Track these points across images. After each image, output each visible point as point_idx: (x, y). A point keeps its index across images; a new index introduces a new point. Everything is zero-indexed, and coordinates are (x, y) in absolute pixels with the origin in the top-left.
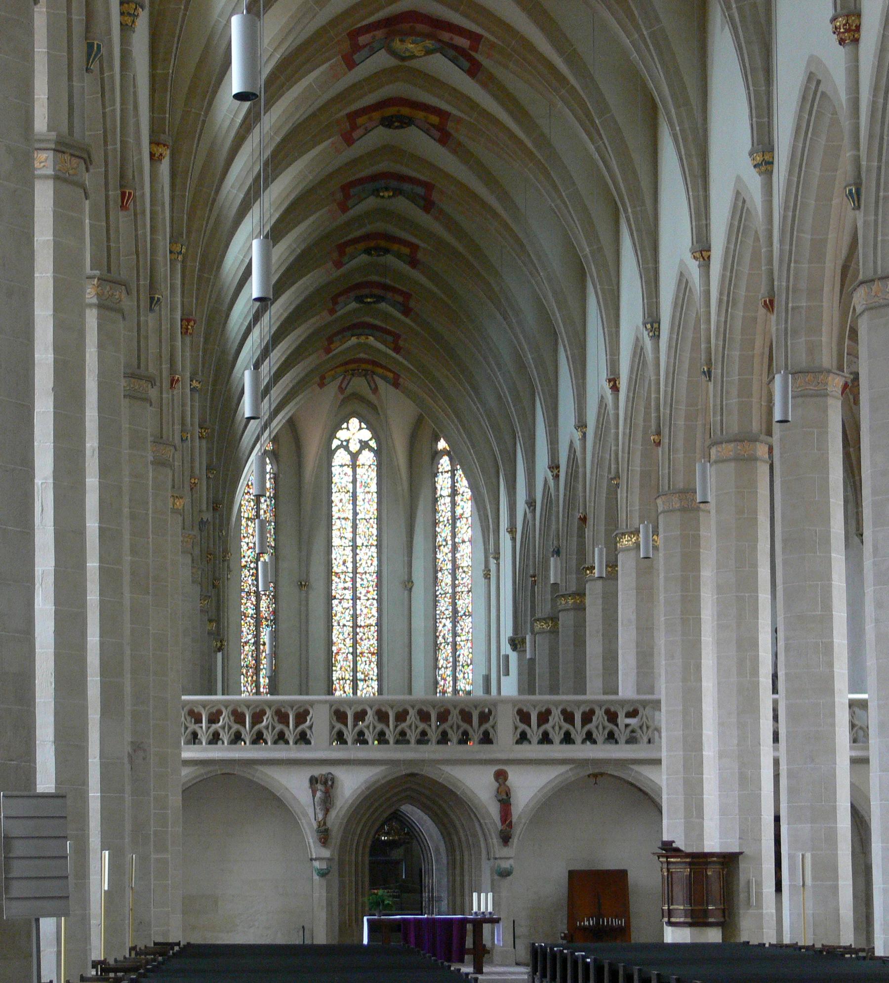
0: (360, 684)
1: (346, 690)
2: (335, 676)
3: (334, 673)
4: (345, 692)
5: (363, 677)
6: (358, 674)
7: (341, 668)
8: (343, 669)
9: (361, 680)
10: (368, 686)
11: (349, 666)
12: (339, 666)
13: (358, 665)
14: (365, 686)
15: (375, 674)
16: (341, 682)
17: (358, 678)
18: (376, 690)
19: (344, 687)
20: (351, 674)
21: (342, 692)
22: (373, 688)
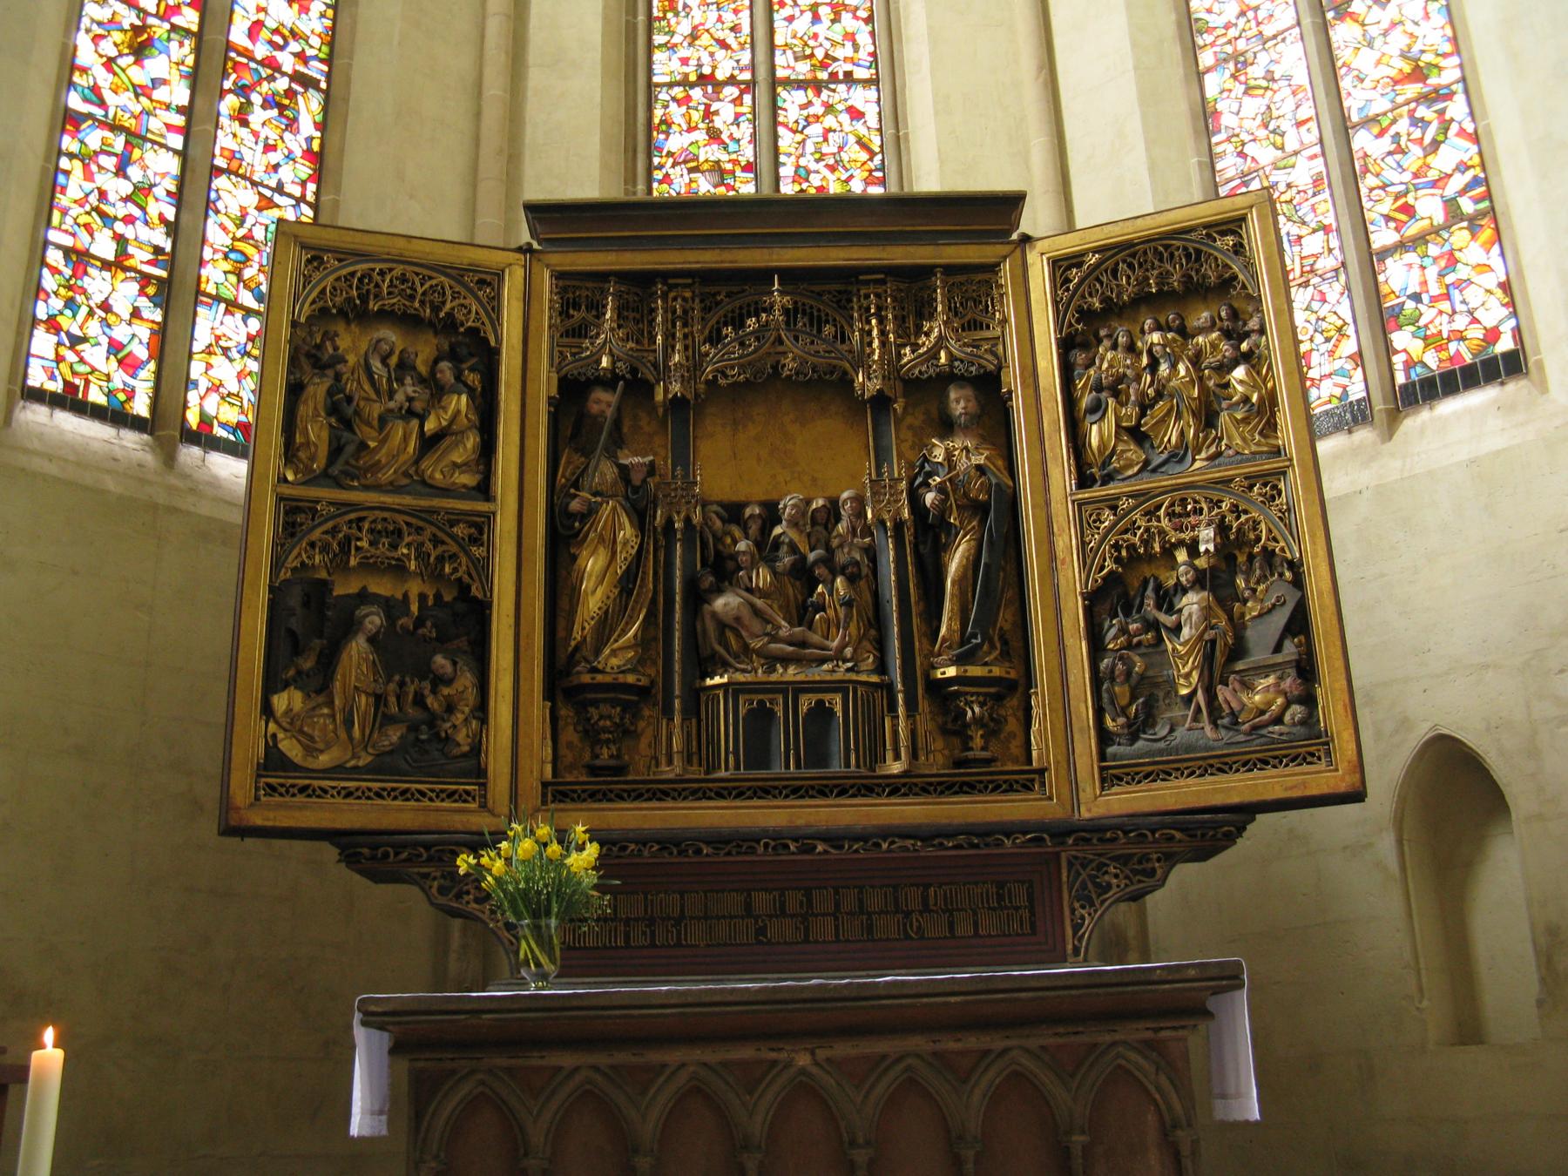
0: (792, 101)
1: (718, 122)
2: (665, 66)
3: (658, 56)
4: (714, 136)
5: (803, 69)
6: (780, 59)
7: (694, 37)
8: (705, 39)
9: (801, 85)
10: (829, 108)
11: (735, 29)
12: (684, 28)
13: (779, 23)
14: (817, 109)
15: (863, 55)
16: (696, 94)
17: (780, 73)
18: (872, 120)
19: (708, 114)
20: (746, 57)
21: (700, 136)
22: (856, 114)
